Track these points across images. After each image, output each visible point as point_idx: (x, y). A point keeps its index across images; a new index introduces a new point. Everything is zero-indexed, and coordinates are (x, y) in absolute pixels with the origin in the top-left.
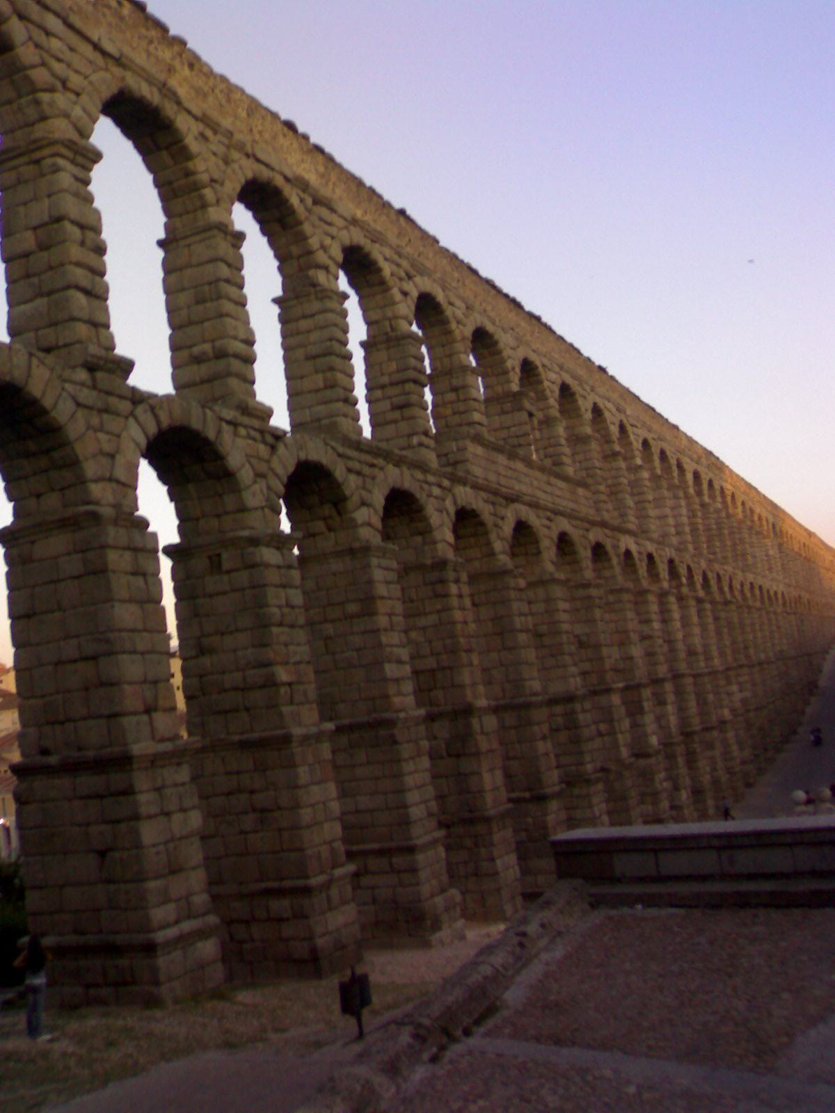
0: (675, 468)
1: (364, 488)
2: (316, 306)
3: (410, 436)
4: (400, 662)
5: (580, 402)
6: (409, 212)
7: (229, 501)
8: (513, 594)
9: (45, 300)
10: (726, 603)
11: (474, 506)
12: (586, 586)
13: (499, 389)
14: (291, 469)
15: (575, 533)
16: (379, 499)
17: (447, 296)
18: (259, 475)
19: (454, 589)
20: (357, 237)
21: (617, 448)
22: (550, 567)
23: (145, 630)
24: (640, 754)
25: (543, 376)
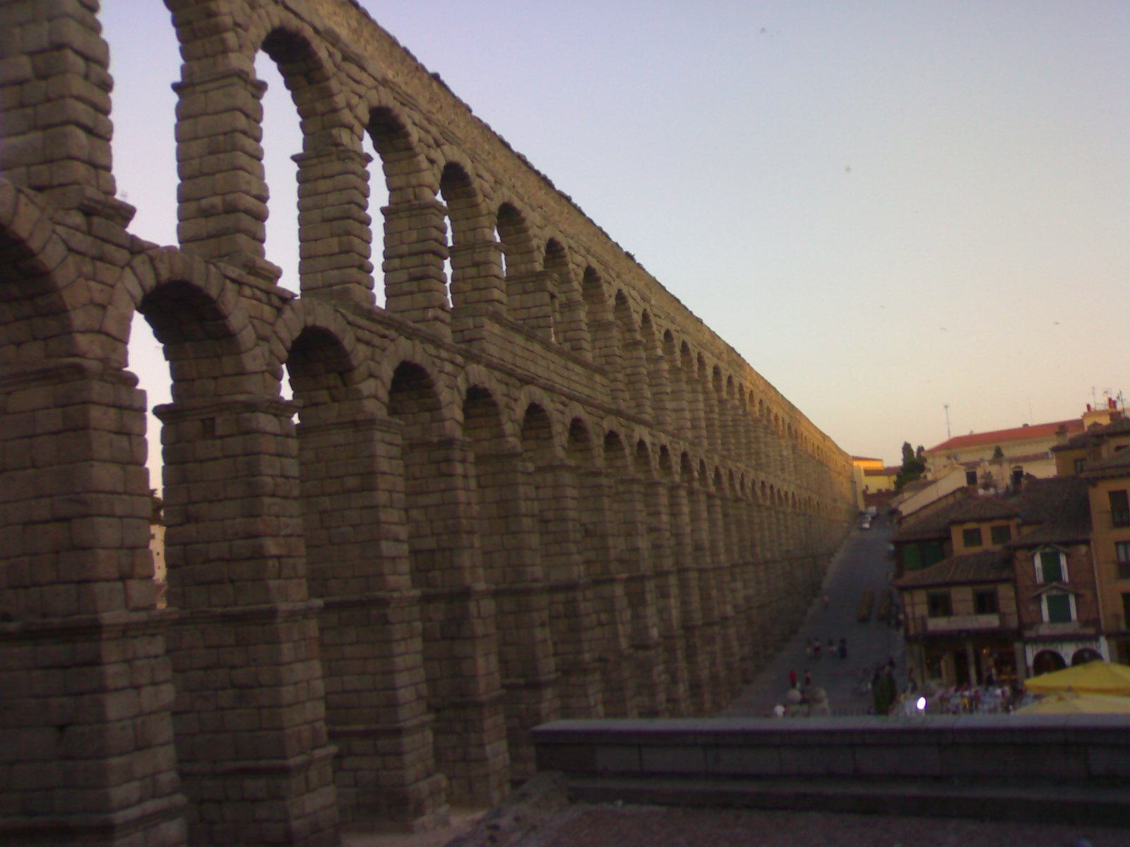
0: (695, 361)
1: (373, 359)
2: (337, 166)
3: (426, 308)
4: (397, 540)
5: (605, 287)
6: (443, 77)
8: (521, 478)
10: (737, 500)
11: (487, 386)
12: (596, 474)
13: (523, 268)
14: (296, 334)
15: (589, 421)
16: (387, 371)
17: (475, 168)
18: (262, 338)
19: (459, 469)
20: (387, 99)
21: (638, 337)
22: (561, 453)
23: (125, 493)
24: (641, 644)
25: (569, 258)
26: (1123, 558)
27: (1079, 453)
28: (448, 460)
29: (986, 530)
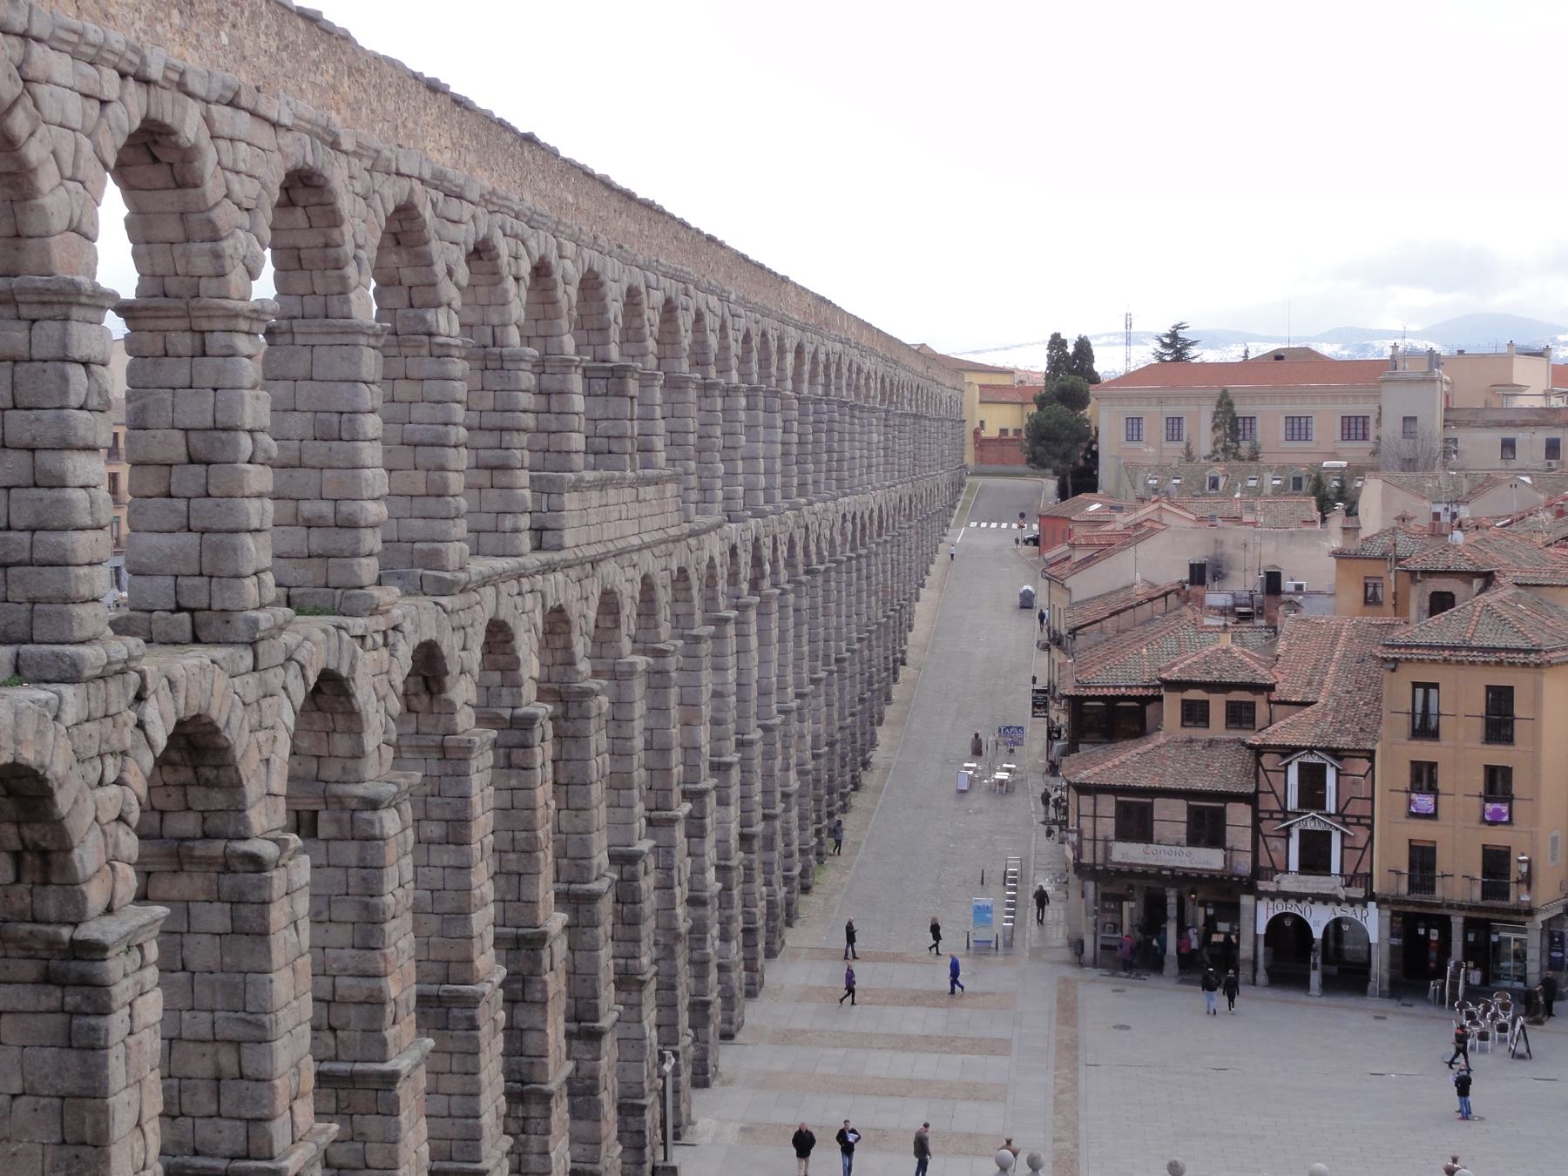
1: (464, 649)
2: (429, 366)
7: (342, 744)
9: (195, 537)
16: (476, 654)
17: (560, 247)
22: (626, 645)
28: (526, 746)
29: (1218, 705)
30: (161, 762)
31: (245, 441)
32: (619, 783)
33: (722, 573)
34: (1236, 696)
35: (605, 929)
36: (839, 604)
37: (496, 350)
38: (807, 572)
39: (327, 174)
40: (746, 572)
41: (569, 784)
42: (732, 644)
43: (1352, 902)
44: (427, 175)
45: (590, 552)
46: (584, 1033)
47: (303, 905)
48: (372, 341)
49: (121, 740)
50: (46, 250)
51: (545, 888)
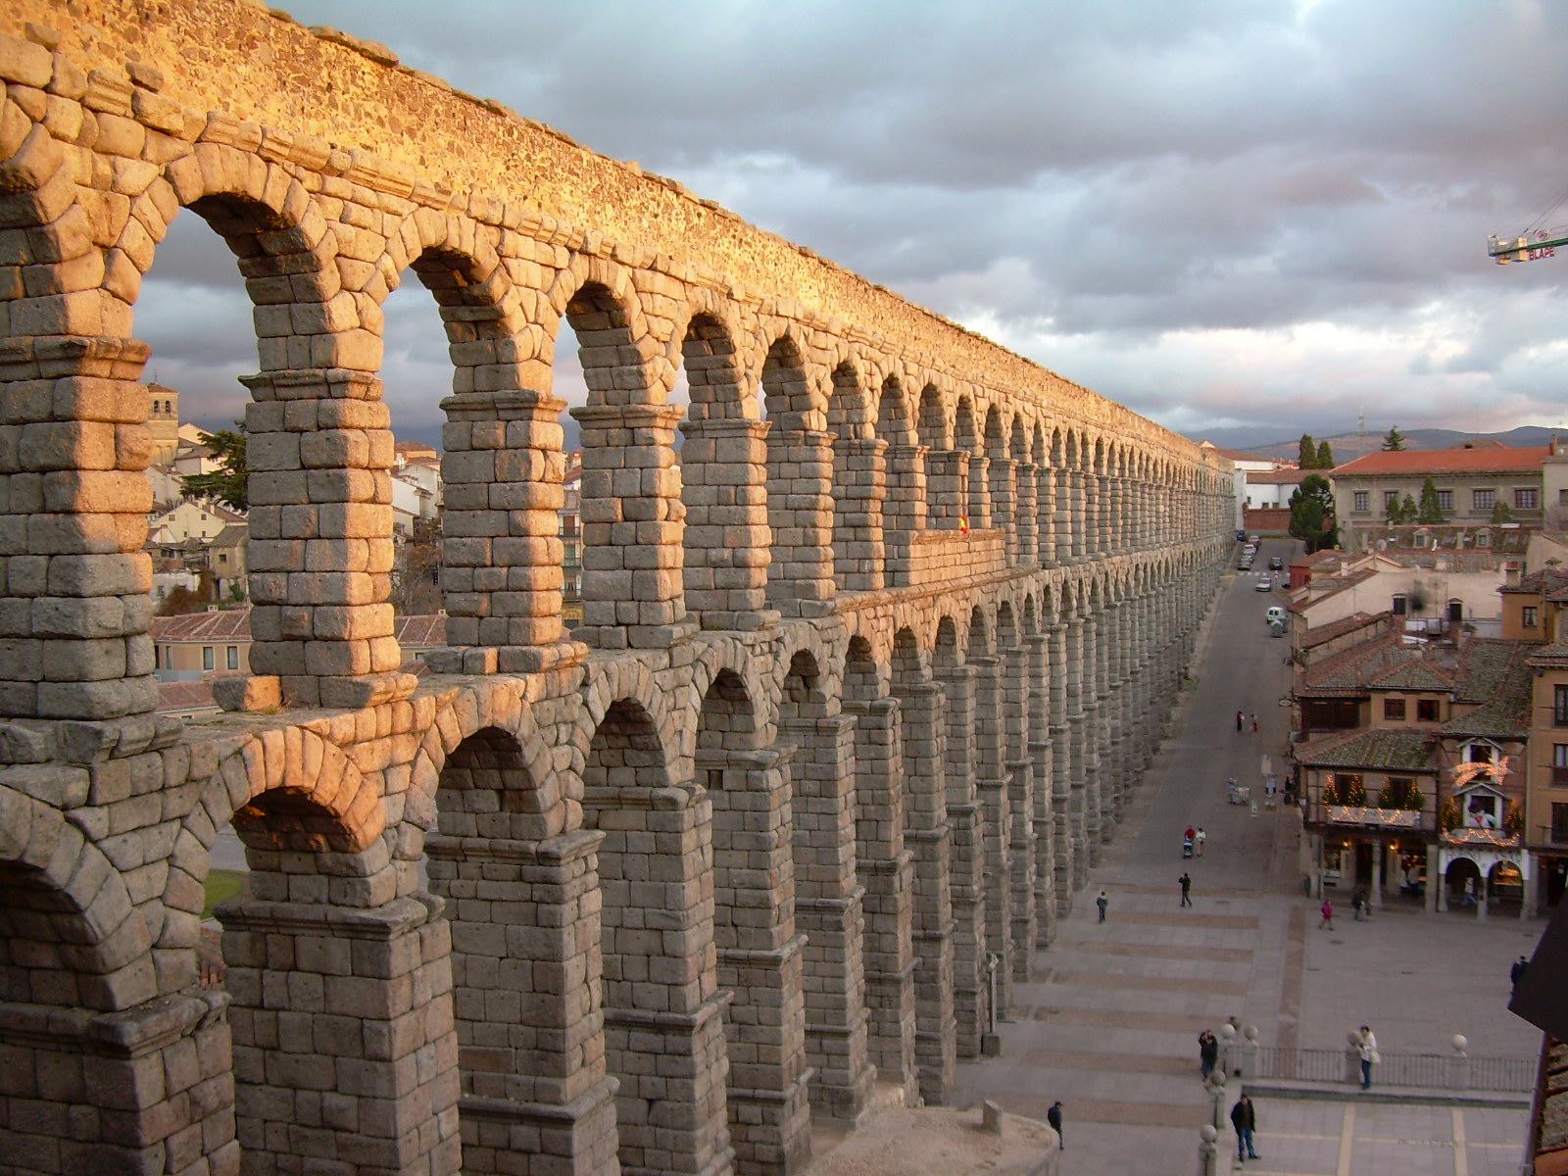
1: (832, 656)
2: (802, 452)
7: (739, 721)
9: (629, 573)
17: (905, 367)
22: (961, 658)
26: (1559, 764)
27: (1529, 601)
30: (598, 731)
31: (662, 505)
32: (954, 757)
33: (1038, 606)
34: (1425, 697)
35: (944, 863)
36: (1133, 631)
37: (857, 441)
38: (1107, 607)
39: (723, 315)
40: (1056, 604)
41: (916, 755)
42: (1045, 659)
43: (1511, 850)
44: (800, 316)
45: (931, 588)
46: (927, 937)
47: (707, 835)
48: (758, 434)
49: (571, 713)
50: (515, 372)
51: (895, 832)
